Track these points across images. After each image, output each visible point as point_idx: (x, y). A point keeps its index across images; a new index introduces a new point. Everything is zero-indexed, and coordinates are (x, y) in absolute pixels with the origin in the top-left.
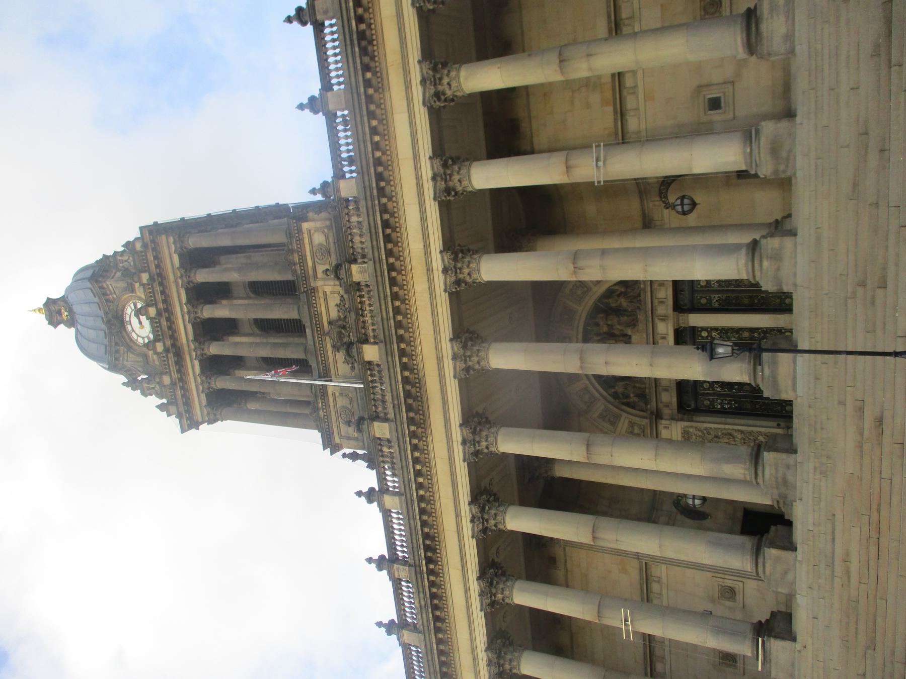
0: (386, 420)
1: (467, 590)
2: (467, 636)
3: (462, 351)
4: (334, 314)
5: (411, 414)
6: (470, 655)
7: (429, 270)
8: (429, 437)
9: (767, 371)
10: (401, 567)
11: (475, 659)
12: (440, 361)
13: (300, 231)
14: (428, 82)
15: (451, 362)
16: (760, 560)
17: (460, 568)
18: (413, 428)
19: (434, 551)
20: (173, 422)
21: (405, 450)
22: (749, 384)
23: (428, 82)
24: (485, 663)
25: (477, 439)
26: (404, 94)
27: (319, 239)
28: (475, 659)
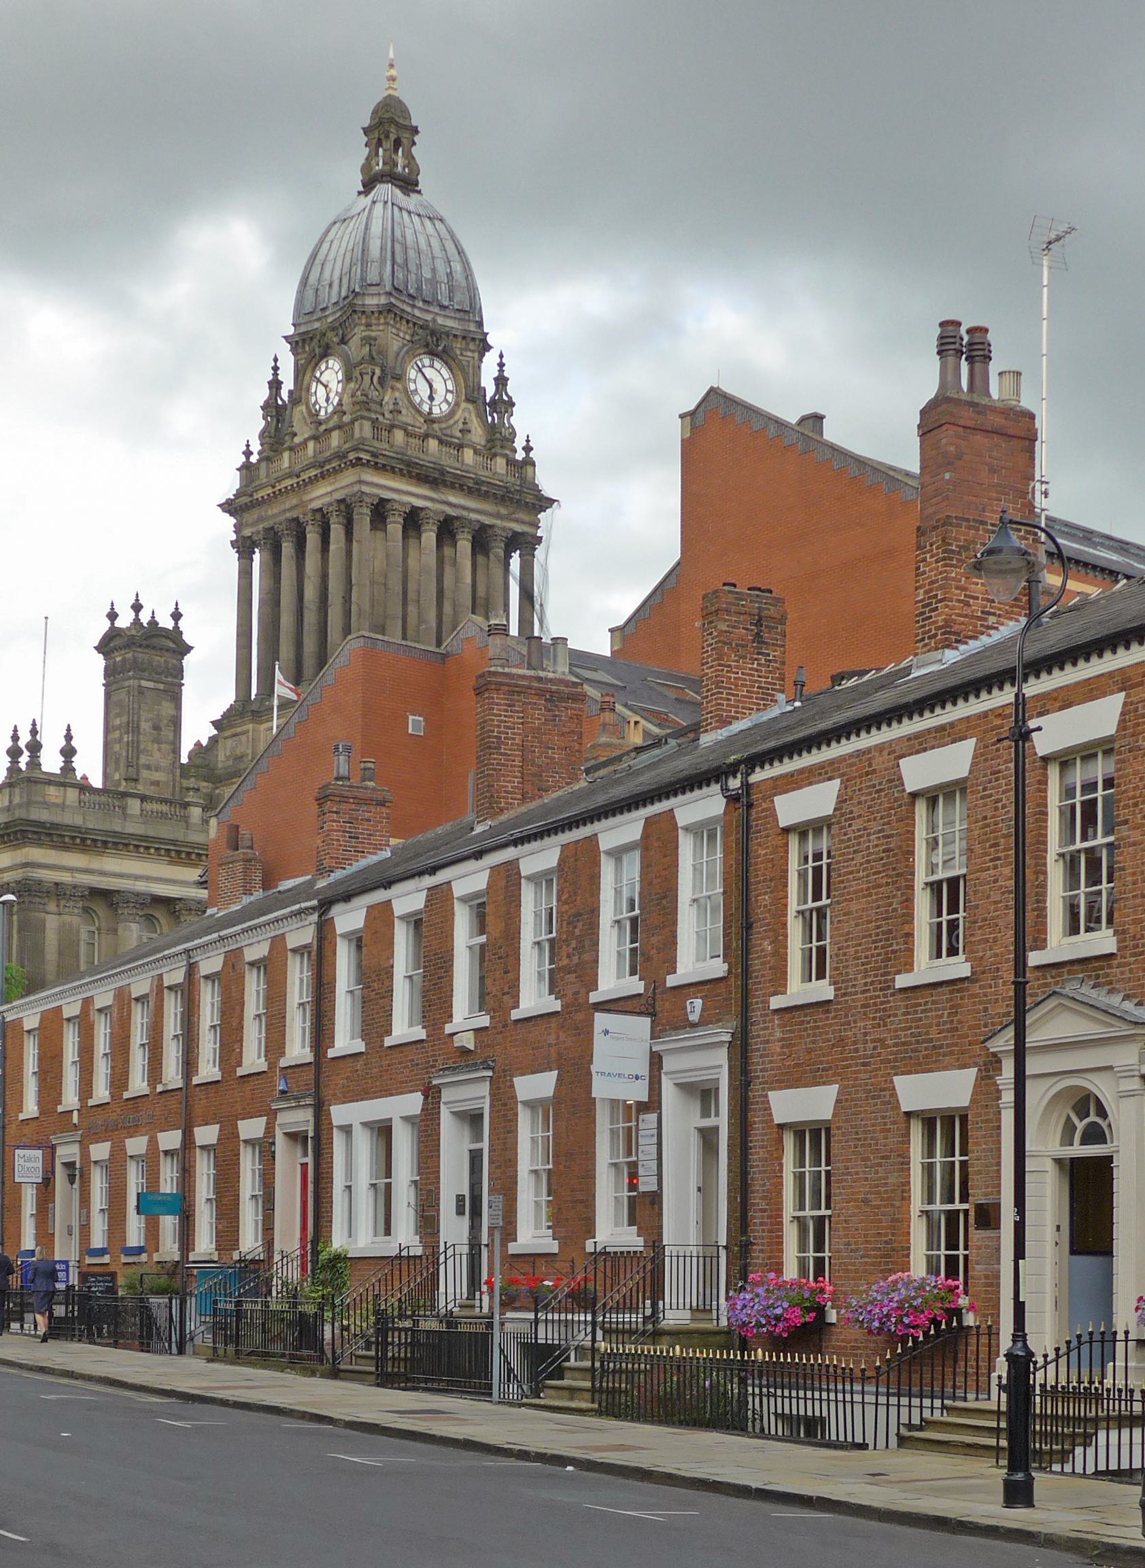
20: (230, 484)
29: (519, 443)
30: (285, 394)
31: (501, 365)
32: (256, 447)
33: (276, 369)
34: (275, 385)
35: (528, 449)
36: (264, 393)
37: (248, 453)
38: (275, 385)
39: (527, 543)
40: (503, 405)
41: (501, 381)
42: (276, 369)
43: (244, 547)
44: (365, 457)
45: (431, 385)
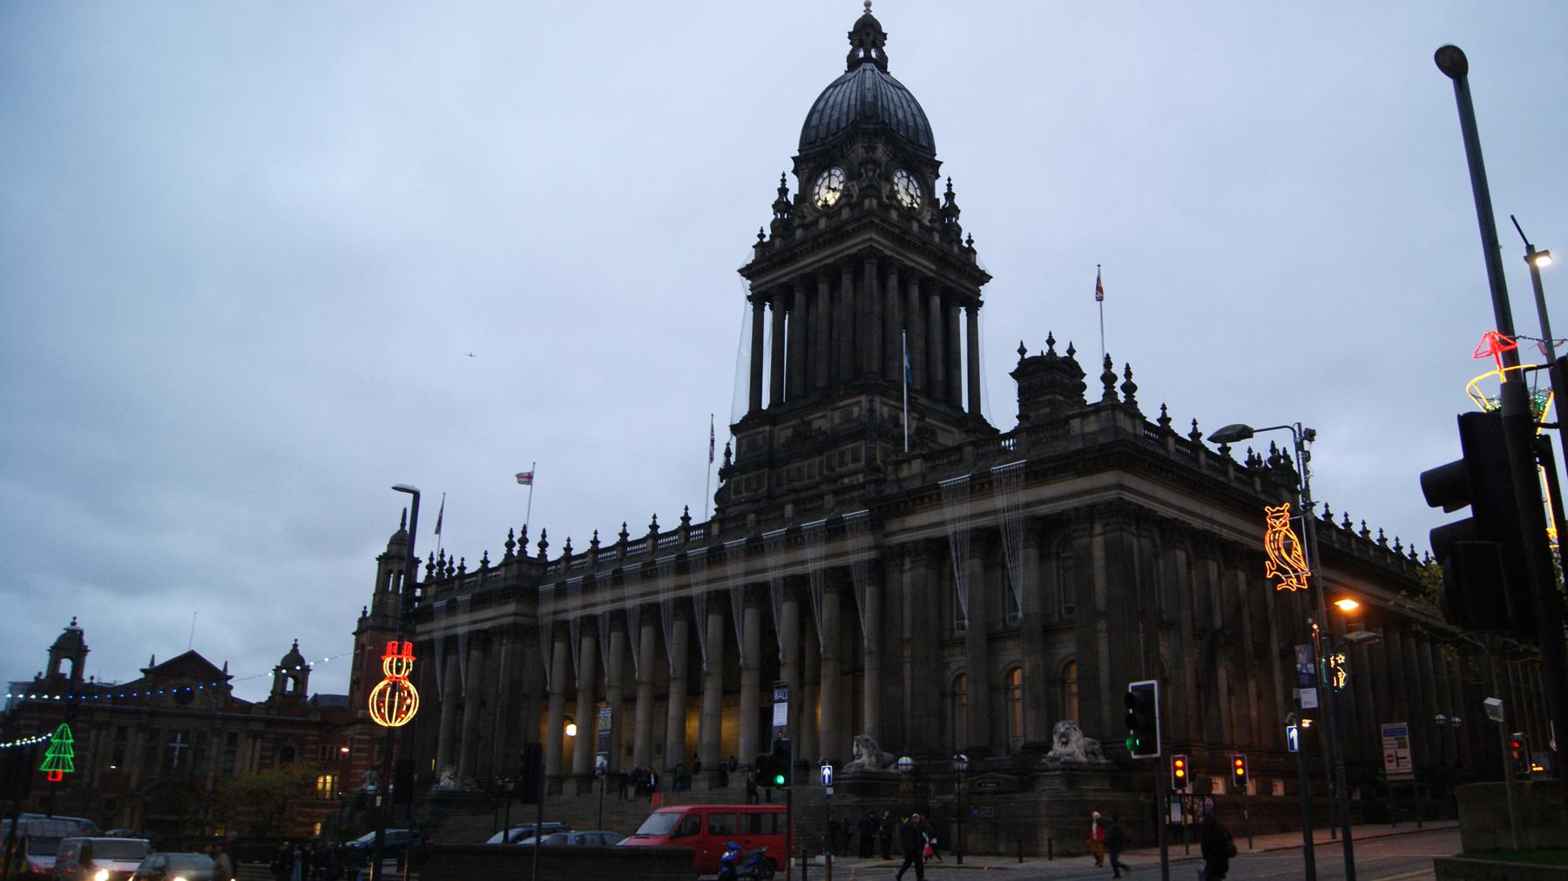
4: (816, 425)
13: (860, 394)
20: (748, 256)
27: (856, 409)
29: (964, 237)
30: (791, 198)
31: (949, 186)
32: (768, 232)
33: (784, 181)
34: (783, 191)
35: (970, 241)
36: (776, 196)
37: (761, 236)
38: (783, 191)
39: (974, 305)
40: (953, 211)
41: (950, 196)
42: (784, 181)
43: (757, 300)
44: (876, 221)
45: (905, 191)
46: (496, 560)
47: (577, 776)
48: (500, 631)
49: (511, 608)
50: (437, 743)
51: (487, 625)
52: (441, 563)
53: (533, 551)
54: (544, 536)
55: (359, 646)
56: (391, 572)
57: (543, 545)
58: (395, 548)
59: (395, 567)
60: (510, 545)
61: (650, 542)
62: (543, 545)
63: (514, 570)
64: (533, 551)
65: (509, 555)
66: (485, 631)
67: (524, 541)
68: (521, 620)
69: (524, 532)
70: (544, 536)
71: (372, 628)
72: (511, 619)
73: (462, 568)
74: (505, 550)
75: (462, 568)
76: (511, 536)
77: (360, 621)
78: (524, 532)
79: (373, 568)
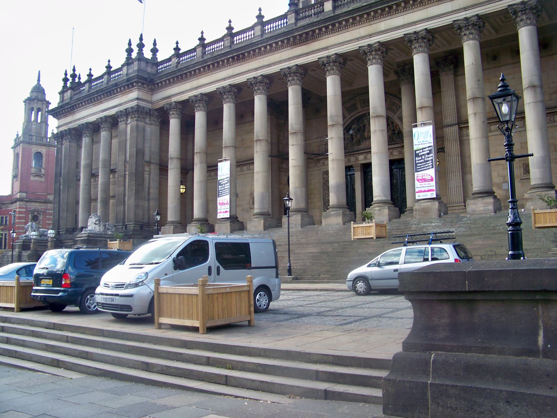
0: (297, 20)
1: (224, 79)
2: (205, 83)
3: (331, 60)
5: (298, 37)
6: (197, 86)
7: (370, 36)
8: (290, 48)
9: (333, 213)
10: (229, 41)
11: (196, 88)
12: (326, 48)
14: (465, 22)
15: (326, 55)
16: (258, 216)
17: (234, 74)
18: (292, 39)
19: (238, 60)
21: (280, 37)
22: (329, 205)
23: (465, 22)
24: (195, 94)
25: (292, 75)
26: (462, 7)
28: (196, 88)
46: (118, 62)
47: (198, 220)
48: (126, 113)
49: (134, 94)
50: (77, 203)
51: (113, 112)
52: (74, 76)
53: (148, 54)
54: (155, 44)
55: (17, 156)
56: (32, 109)
57: (155, 51)
58: (35, 94)
59: (36, 106)
60: (129, 51)
61: (258, 28)
62: (155, 51)
63: (135, 66)
64: (148, 54)
65: (129, 58)
66: (112, 117)
67: (141, 46)
68: (142, 104)
69: (141, 39)
70: (155, 44)
71: (22, 142)
72: (135, 103)
73: (90, 75)
74: (125, 55)
75: (90, 75)
76: (130, 44)
77: (15, 140)
78: (141, 39)
79: (21, 108)
